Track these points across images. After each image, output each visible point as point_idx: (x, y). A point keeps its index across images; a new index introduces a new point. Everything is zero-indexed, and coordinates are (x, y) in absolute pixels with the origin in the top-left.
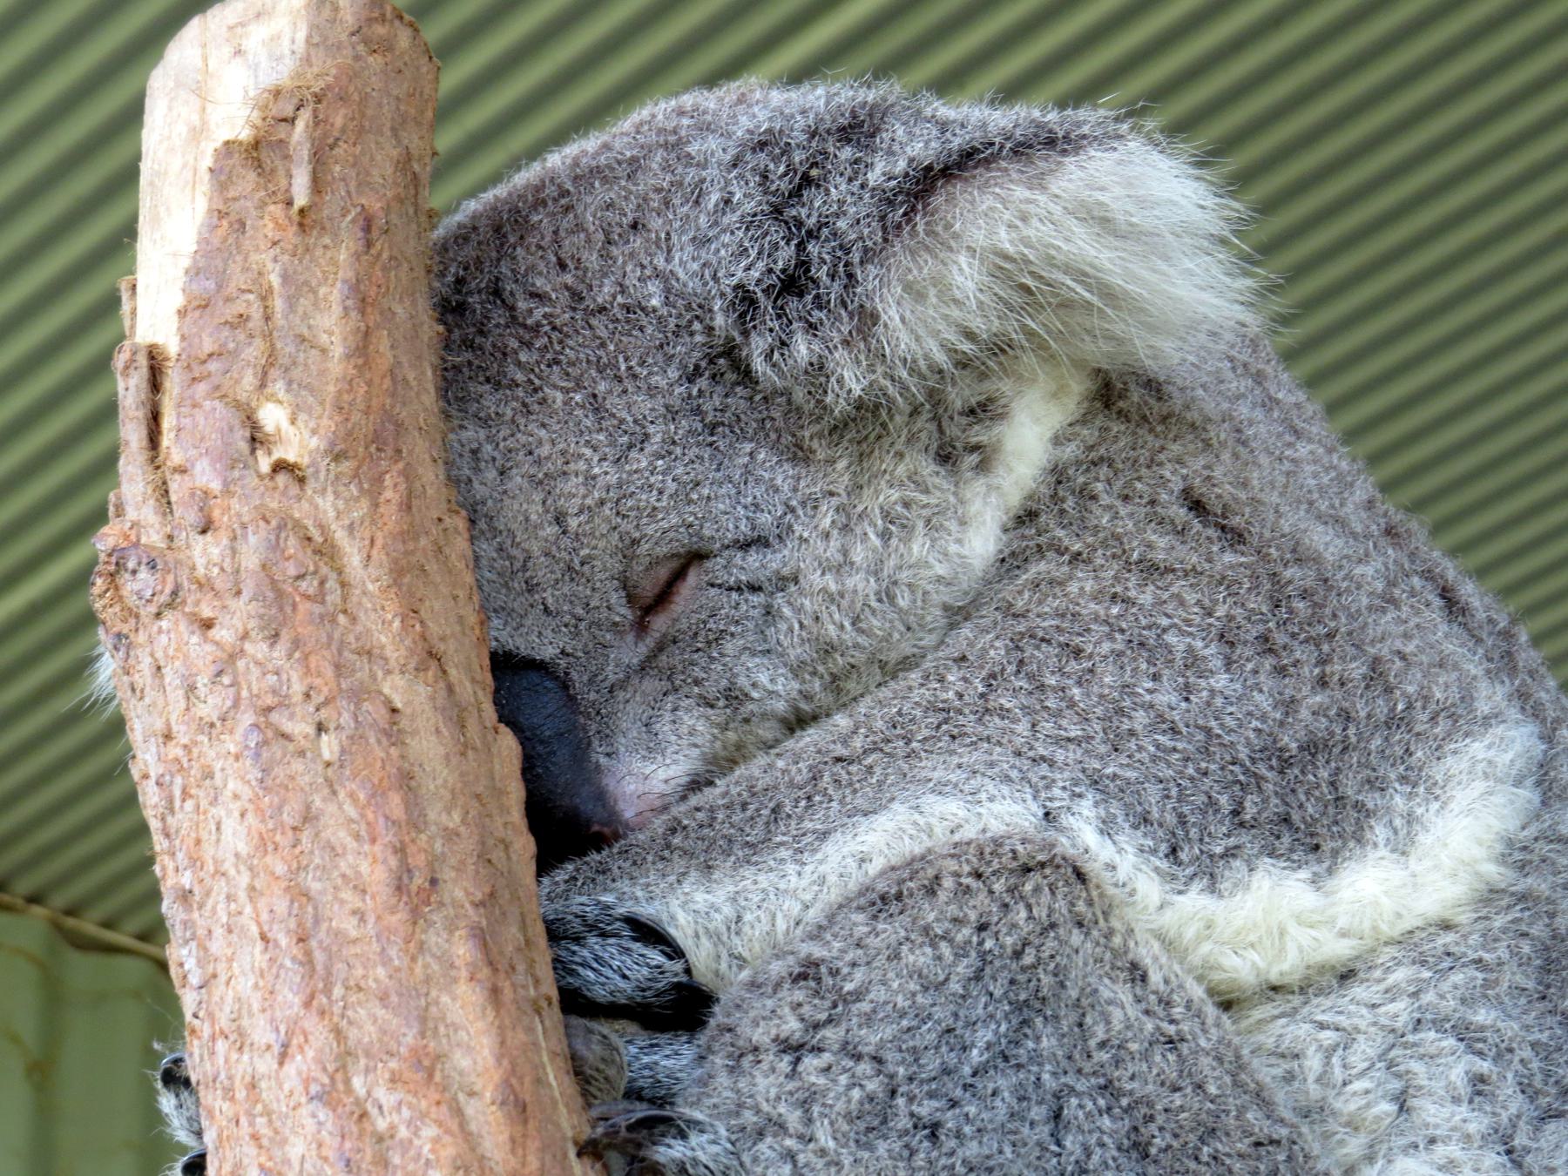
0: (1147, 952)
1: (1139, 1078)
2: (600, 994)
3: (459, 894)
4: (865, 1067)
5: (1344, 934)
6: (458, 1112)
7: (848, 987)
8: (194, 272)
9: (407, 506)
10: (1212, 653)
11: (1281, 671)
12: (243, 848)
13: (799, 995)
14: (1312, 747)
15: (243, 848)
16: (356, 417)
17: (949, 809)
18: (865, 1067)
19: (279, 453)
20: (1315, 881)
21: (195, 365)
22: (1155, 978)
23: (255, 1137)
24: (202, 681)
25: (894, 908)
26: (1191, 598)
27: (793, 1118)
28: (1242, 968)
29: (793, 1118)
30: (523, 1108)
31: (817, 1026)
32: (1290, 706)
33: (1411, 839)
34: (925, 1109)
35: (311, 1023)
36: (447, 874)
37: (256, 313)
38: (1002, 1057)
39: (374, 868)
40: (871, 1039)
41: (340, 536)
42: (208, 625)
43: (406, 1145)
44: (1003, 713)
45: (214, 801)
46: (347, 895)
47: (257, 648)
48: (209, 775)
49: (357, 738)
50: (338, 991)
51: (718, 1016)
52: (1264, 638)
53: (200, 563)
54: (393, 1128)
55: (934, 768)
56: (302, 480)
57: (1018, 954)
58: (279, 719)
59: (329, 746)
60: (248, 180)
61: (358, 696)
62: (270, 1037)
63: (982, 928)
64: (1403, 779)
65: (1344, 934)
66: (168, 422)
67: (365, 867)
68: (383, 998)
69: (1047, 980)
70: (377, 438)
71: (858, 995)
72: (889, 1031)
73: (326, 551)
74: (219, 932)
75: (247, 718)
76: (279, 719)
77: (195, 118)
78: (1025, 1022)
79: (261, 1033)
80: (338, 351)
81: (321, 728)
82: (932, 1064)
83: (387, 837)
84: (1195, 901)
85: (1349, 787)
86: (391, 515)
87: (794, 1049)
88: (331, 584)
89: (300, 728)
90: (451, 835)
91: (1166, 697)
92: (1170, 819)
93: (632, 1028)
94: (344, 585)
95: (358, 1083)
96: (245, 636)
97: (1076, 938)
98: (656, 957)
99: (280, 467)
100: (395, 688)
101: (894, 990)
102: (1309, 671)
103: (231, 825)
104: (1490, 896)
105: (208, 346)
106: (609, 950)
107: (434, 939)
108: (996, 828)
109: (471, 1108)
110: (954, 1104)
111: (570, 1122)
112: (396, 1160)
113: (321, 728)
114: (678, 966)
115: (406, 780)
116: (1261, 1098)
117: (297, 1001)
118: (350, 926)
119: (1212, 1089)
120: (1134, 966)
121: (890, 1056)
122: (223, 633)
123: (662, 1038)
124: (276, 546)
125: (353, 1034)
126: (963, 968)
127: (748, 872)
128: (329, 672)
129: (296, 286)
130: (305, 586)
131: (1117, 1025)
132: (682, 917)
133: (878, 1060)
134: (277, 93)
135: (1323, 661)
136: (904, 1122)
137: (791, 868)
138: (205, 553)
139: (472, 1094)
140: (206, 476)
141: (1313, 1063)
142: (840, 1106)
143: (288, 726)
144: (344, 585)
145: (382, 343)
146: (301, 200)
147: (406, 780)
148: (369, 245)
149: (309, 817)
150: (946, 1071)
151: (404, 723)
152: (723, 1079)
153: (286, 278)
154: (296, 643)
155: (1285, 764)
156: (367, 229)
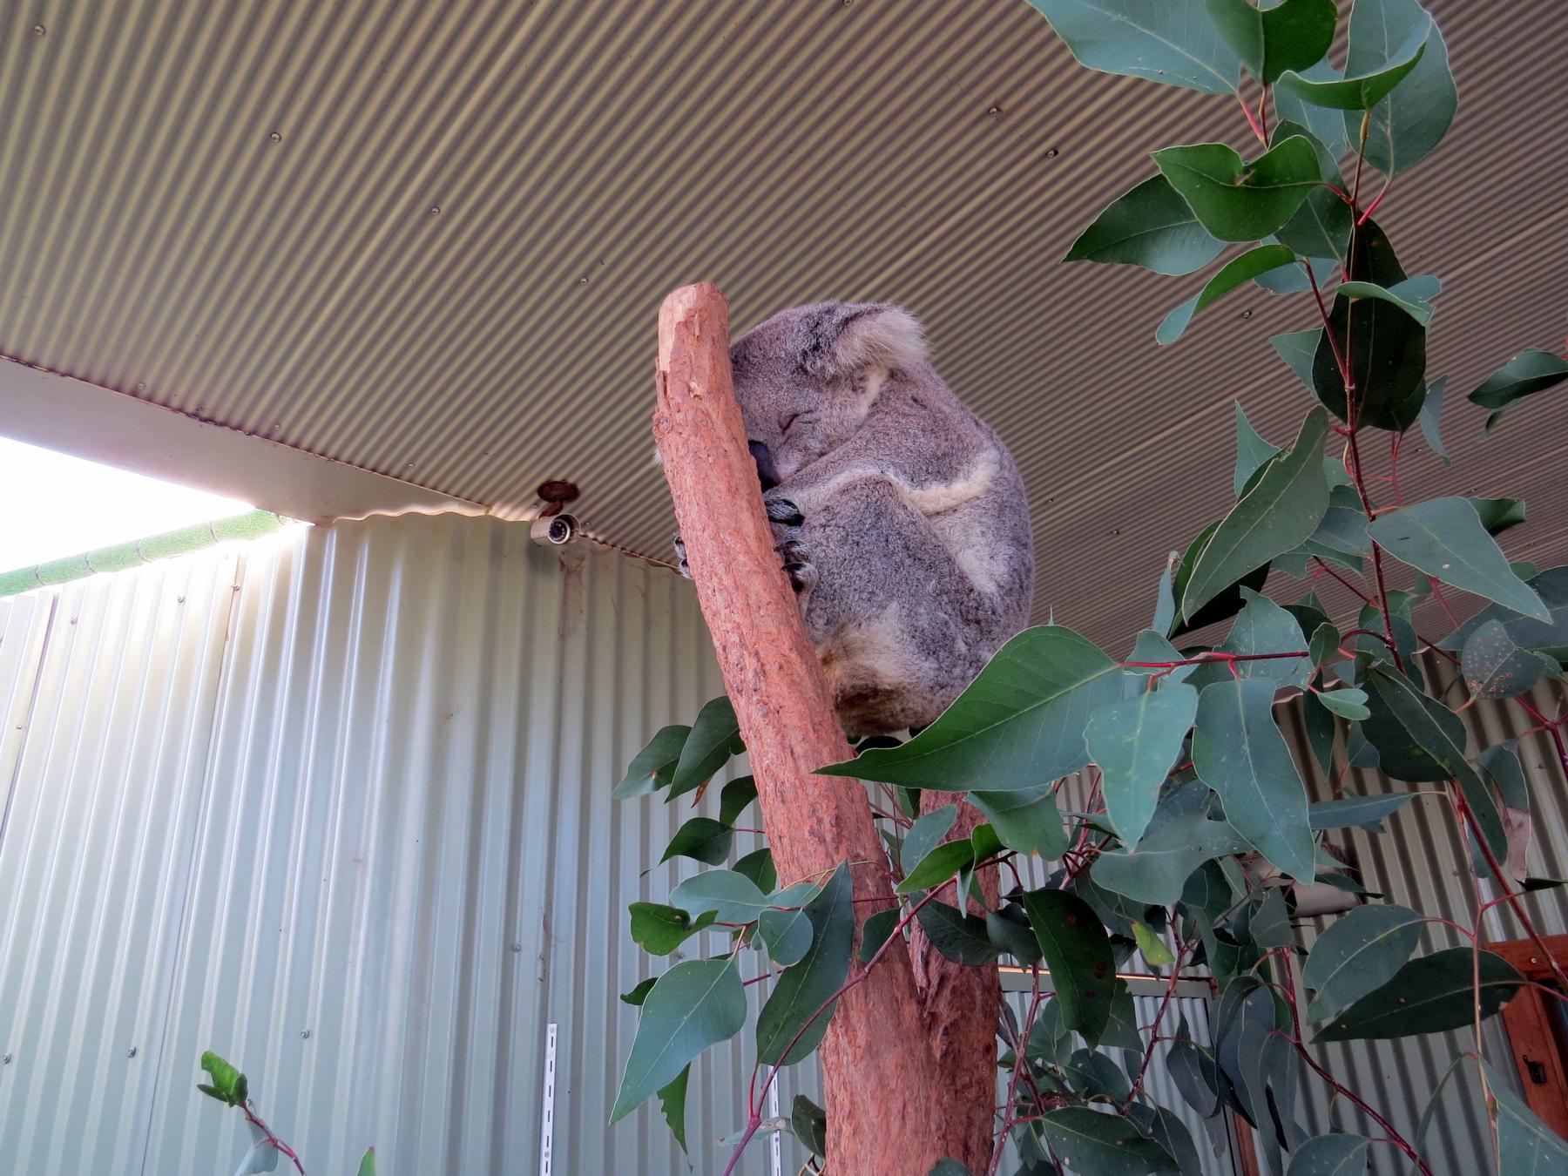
0: (907, 503)
1: (907, 531)
2: (778, 517)
3: (743, 492)
4: (841, 529)
5: (953, 499)
6: (746, 541)
7: (836, 511)
8: (672, 353)
9: (726, 404)
10: (920, 433)
11: (937, 437)
12: (692, 484)
13: (825, 514)
14: (944, 455)
15: (692, 484)
16: (713, 384)
17: (860, 471)
18: (841, 529)
19: (695, 393)
20: (946, 487)
21: (674, 374)
22: (909, 508)
23: (698, 550)
24: (680, 447)
25: (846, 492)
26: (914, 421)
27: (825, 542)
28: (930, 507)
29: (825, 542)
30: (760, 539)
31: (829, 521)
32: (939, 445)
33: (969, 477)
34: (856, 538)
35: (710, 523)
36: (739, 488)
37: (688, 361)
38: (873, 526)
39: (722, 486)
40: (842, 523)
41: (711, 411)
42: (681, 433)
43: (733, 549)
44: (871, 449)
45: (684, 474)
46: (716, 493)
47: (693, 438)
48: (682, 468)
50: (716, 515)
51: (806, 521)
52: (932, 430)
53: (678, 419)
54: (730, 546)
55: (855, 462)
56: (701, 399)
57: (876, 503)
58: (699, 454)
59: (711, 460)
60: (684, 331)
61: (717, 448)
62: (700, 527)
63: (867, 497)
64: (967, 462)
65: (953, 499)
66: (668, 389)
67: (721, 487)
68: (726, 516)
69: (883, 508)
70: (718, 389)
71: (838, 513)
72: (846, 521)
73: (708, 415)
74: (687, 504)
76: (699, 454)
77: (671, 317)
78: (879, 518)
79: (698, 526)
80: (708, 369)
81: (708, 456)
82: (857, 528)
83: (725, 479)
84: (918, 491)
85: (954, 464)
86: (723, 406)
87: (824, 526)
88: (709, 422)
89: (704, 456)
90: (740, 479)
91: (909, 444)
92: (911, 472)
93: (785, 525)
94: (712, 423)
95: (721, 535)
96: (690, 435)
97: (890, 498)
98: (791, 508)
99: (696, 396)
100: (726, 446)
101: (847, 511)
102: (943, 437)
103: (688, 480)
104: (989, 491)
105: (677, 369)
106: (779, 507)
107: (738, 502)
108: (869, 475)
109: (748, 540)
110: (862, 537)
111: (772, 544)
112: (731, 552)
113: (708, 456)
114: (796, 510)
115: (729, 467)
116: (935, 536)
117: (706, 518)
118: (718, 500)
119: (924, 533)
120: (904, 506)
121: (847, 527)
122: (684, 435)
123: (793, 527)
125: (719, 524)
126: (863, 506)
127: (811, 488)
128: (710, 442)
130: (704, 423)
131: (900, 518)
132: (796, 500)
133: (844, 527)
134: (690, 310)
135: (947, 435)
136: (851, 542)
137: (822, 487)
138: (679, 417)
139: (749, 537)
140: (678, 399)
141: (948, 530)
142: (835, 538)
143: (701, 455)
144: (712, 423)
145: (718, 366)
146: (697, 334)
147: (729, 467)
148: (714, 344)
150: (860, 530)
151: (728, 453)
152: (808, 535)
153: (694, 353)
154: (702, 436)
155: (938, 459)
156: (714, 340)
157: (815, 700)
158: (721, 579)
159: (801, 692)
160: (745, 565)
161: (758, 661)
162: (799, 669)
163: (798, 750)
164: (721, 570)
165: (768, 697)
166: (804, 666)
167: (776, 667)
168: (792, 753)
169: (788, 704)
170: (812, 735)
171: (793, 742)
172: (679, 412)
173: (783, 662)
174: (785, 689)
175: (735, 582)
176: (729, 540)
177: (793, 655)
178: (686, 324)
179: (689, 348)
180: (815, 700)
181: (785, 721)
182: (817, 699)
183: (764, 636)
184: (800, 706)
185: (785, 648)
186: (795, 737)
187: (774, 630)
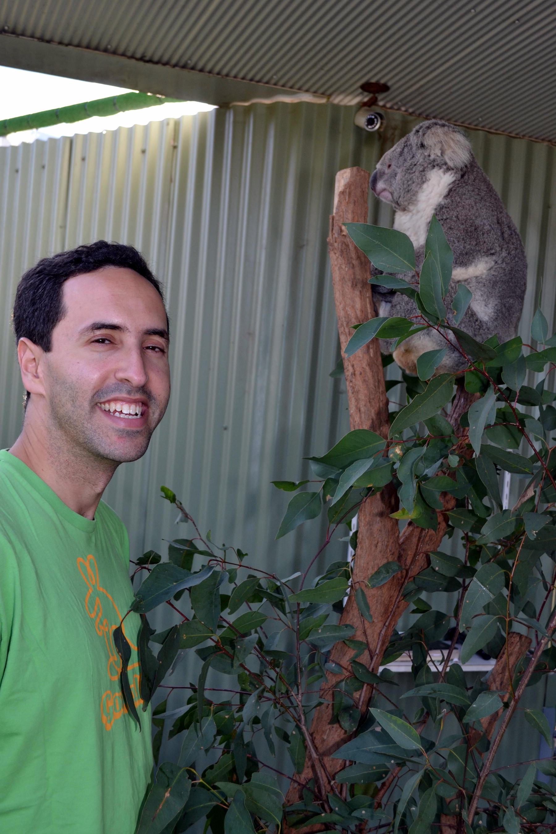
6: (356, 312)
30: (363, 312)
41: (349, 243)
47: (340, 257)
58: (342, 266)
59: (347, 269)
73: (347, 246)
75: (339, 266)
76: (342, 266)
89: (344, 267)
95: (347, 308)
99: (343, 235)
118: (347, 290)
124: (342, 245)
130: (345, 250)
144: (349, 250)
153: (346, 210)
157: (373, 388)
158: (344, 329)
159: (367, 385)
161: (353, 369)
162: (368, 374)
163: (362, 409)
164: (345, 325)
165: (355, 385)
166: (371, 373)
167: (359, 373)
168: (360, 411)
169: (361, 389)
170: (368, 404)
171: (361, 406)
172: (336, 242)
174: (361, 383)
175: (349, 332)
177: (367, 369)
180: (373, 388)
181: (360, 396)
182: (374, 388)
183: (357, 358)
184: (366, 392)
185: (364, 365)
187: (361, 355)
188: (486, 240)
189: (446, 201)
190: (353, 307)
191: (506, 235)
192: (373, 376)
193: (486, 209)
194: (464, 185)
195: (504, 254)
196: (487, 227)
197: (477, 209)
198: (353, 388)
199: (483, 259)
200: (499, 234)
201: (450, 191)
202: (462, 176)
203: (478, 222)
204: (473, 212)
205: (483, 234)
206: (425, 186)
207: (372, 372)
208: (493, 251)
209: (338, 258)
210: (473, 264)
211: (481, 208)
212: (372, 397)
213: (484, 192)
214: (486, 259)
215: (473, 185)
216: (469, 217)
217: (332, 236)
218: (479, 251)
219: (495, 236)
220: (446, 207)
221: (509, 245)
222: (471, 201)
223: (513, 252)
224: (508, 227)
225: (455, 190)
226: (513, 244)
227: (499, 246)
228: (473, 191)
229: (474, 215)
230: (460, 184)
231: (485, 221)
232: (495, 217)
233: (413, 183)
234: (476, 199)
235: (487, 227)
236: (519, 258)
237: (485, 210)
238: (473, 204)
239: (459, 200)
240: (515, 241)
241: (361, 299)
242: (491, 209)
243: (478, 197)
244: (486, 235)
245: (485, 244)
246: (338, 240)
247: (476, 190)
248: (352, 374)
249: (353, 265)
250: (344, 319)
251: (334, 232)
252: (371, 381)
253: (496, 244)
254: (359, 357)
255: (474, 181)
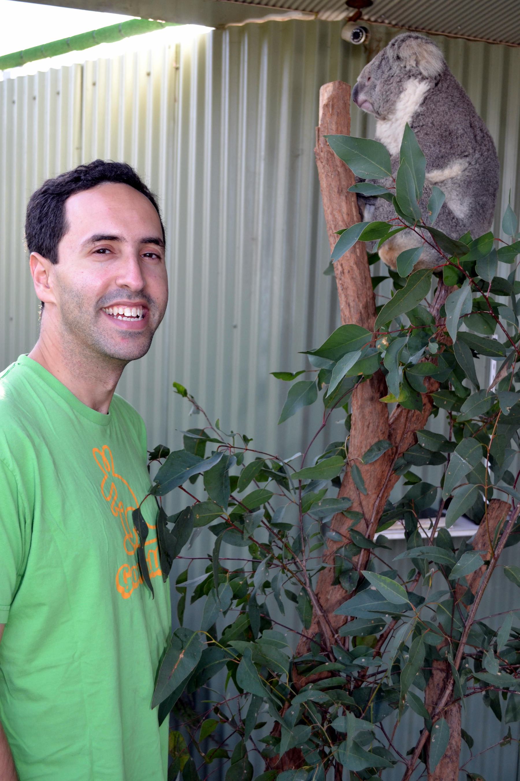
6: (342, 215)
36: (344, 190)
47: (326, 165)
49: (335, 176)
60: (326, 109)
61: (335, 171)
73: (332, 155)
75: (325, 173)
89: (330, 175)
90: (344, 185)
100: (339, 169)
122: (323, 164)
124: (327, 155)
129: (331, 123)
138: (322, 154)
145: (340, 128)
149: (330, 184)
159: (355, 282)
160: (341, 226)
161: (342, 267)
163: (352, 304)
164: (333, 228)
167: (347, 271)
168: (349, 306)
169: (350, 287)
170: (357, 299)
173: (350, 270)
176: (337, 215)
177: (355, 267)
178: (326, 106)
179: (327, 119)
181: (348, 293)
184: (354, 288)
185: (352, 263)
186: (351, 299)
188: (460, 143)
189: (422, 109)
190: (340, 211)
191: (478, 138)
192: (360, 274)
193: (460, 114)
194: (438, 92)
195: (477, 155)
196: (460, 131)
197: (451, 115)
198: (343, 285)
199: (457, 161)
200: (472, 137)
201: (425, 99)
202: (436, 85)
203: (452, 127)
204: (447, 117)
205: (457, 138)
206: (402, 96)
207: (359, 269)
208: (466, 154)
209: (324, 166)
210: (448, 166)
211: (454, 114)
212: (360, 293)
213: (458, 99)
214: (461, 161)
215: (446, 92)
216: (443, 123)
217: (319, 146)
218: (454, 154)
219: (468, 139)
220: (422, 115)
221: (482, 147)
222: (446, 108)
223: (486, 153)
224: (481, 130)
225: (430, 98)
226: (485, 145)
227: (472, 148)
228: (447, 98)
229: (448, 120)
230: (435, 93)
231: (459, 126)
232: (468, 121)
233: (391, 93)
234: (450, 105)
235: (460, 131)
236: (491, 159)
237: (458, 115)
238: (447, 110)
239: (434, 107)
240: (487, 143)
241: (347, 203)
242: (464, 114)
243: (452, 104)
244: (459, 139)
245: (459, 148)
246: (324, 150)
247: (450, 97)
248: (341, 273)
249: (339, 172)
250: (332, 222)
251: (320, 142)
252: (358, 278)
253: (469, 147)
254: (347, 257)
255: (448, 87)
